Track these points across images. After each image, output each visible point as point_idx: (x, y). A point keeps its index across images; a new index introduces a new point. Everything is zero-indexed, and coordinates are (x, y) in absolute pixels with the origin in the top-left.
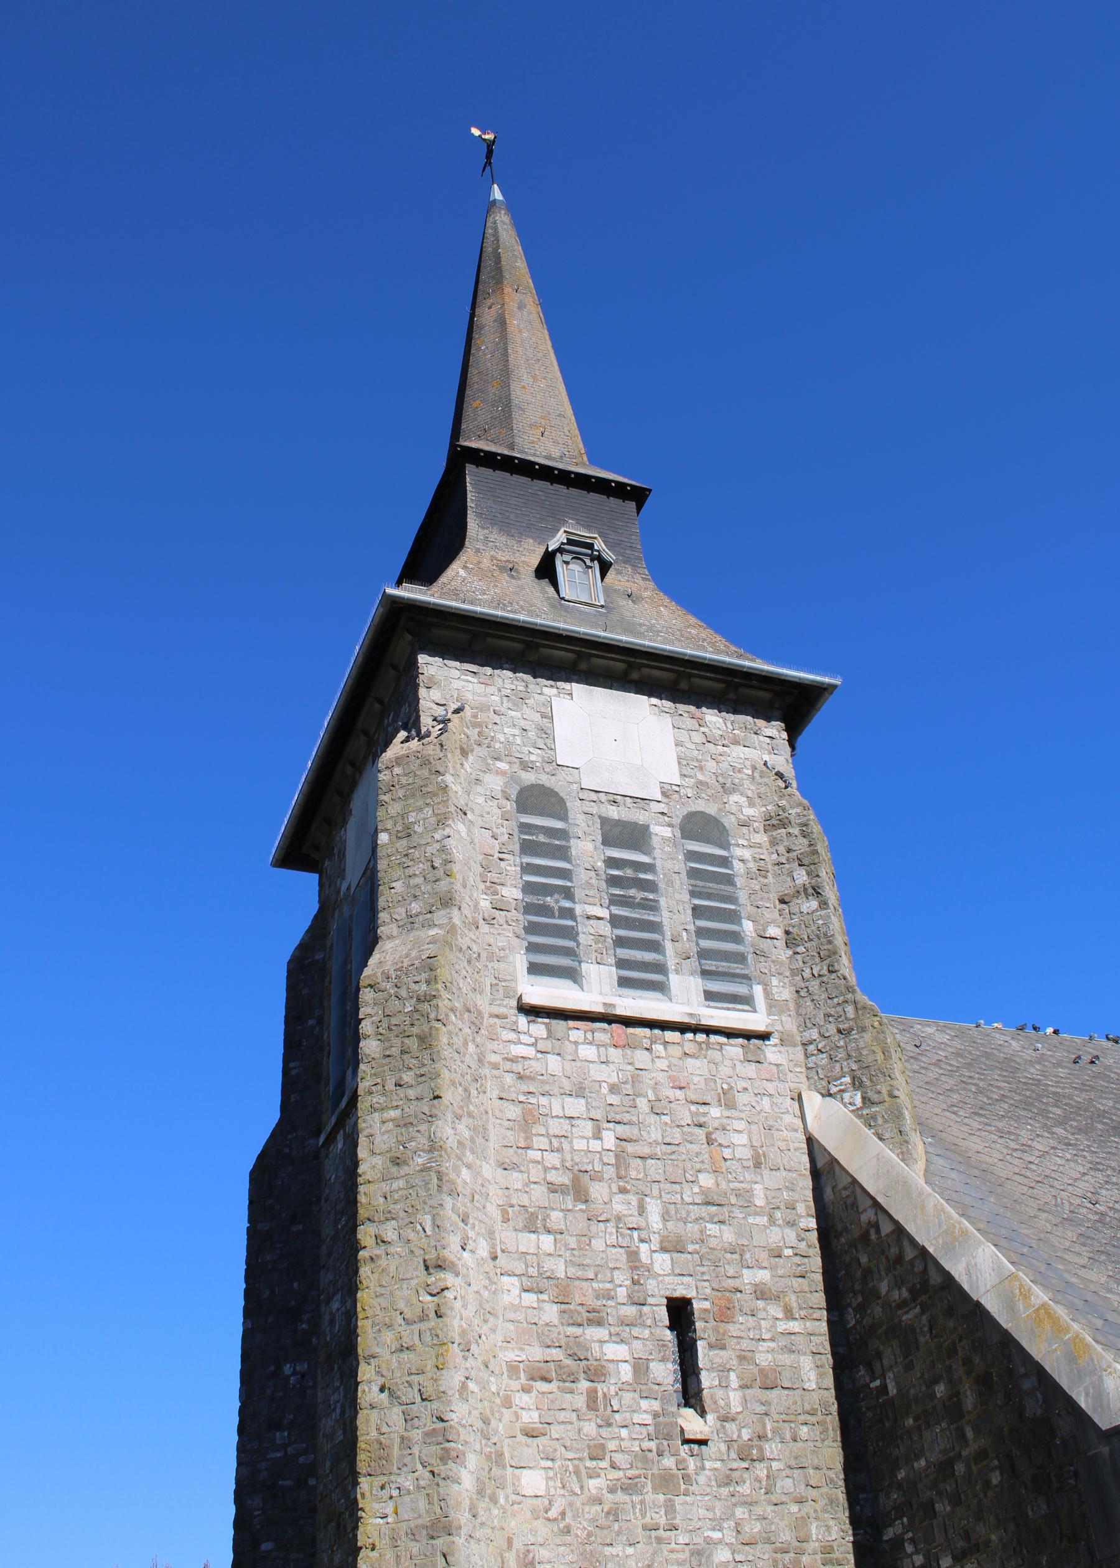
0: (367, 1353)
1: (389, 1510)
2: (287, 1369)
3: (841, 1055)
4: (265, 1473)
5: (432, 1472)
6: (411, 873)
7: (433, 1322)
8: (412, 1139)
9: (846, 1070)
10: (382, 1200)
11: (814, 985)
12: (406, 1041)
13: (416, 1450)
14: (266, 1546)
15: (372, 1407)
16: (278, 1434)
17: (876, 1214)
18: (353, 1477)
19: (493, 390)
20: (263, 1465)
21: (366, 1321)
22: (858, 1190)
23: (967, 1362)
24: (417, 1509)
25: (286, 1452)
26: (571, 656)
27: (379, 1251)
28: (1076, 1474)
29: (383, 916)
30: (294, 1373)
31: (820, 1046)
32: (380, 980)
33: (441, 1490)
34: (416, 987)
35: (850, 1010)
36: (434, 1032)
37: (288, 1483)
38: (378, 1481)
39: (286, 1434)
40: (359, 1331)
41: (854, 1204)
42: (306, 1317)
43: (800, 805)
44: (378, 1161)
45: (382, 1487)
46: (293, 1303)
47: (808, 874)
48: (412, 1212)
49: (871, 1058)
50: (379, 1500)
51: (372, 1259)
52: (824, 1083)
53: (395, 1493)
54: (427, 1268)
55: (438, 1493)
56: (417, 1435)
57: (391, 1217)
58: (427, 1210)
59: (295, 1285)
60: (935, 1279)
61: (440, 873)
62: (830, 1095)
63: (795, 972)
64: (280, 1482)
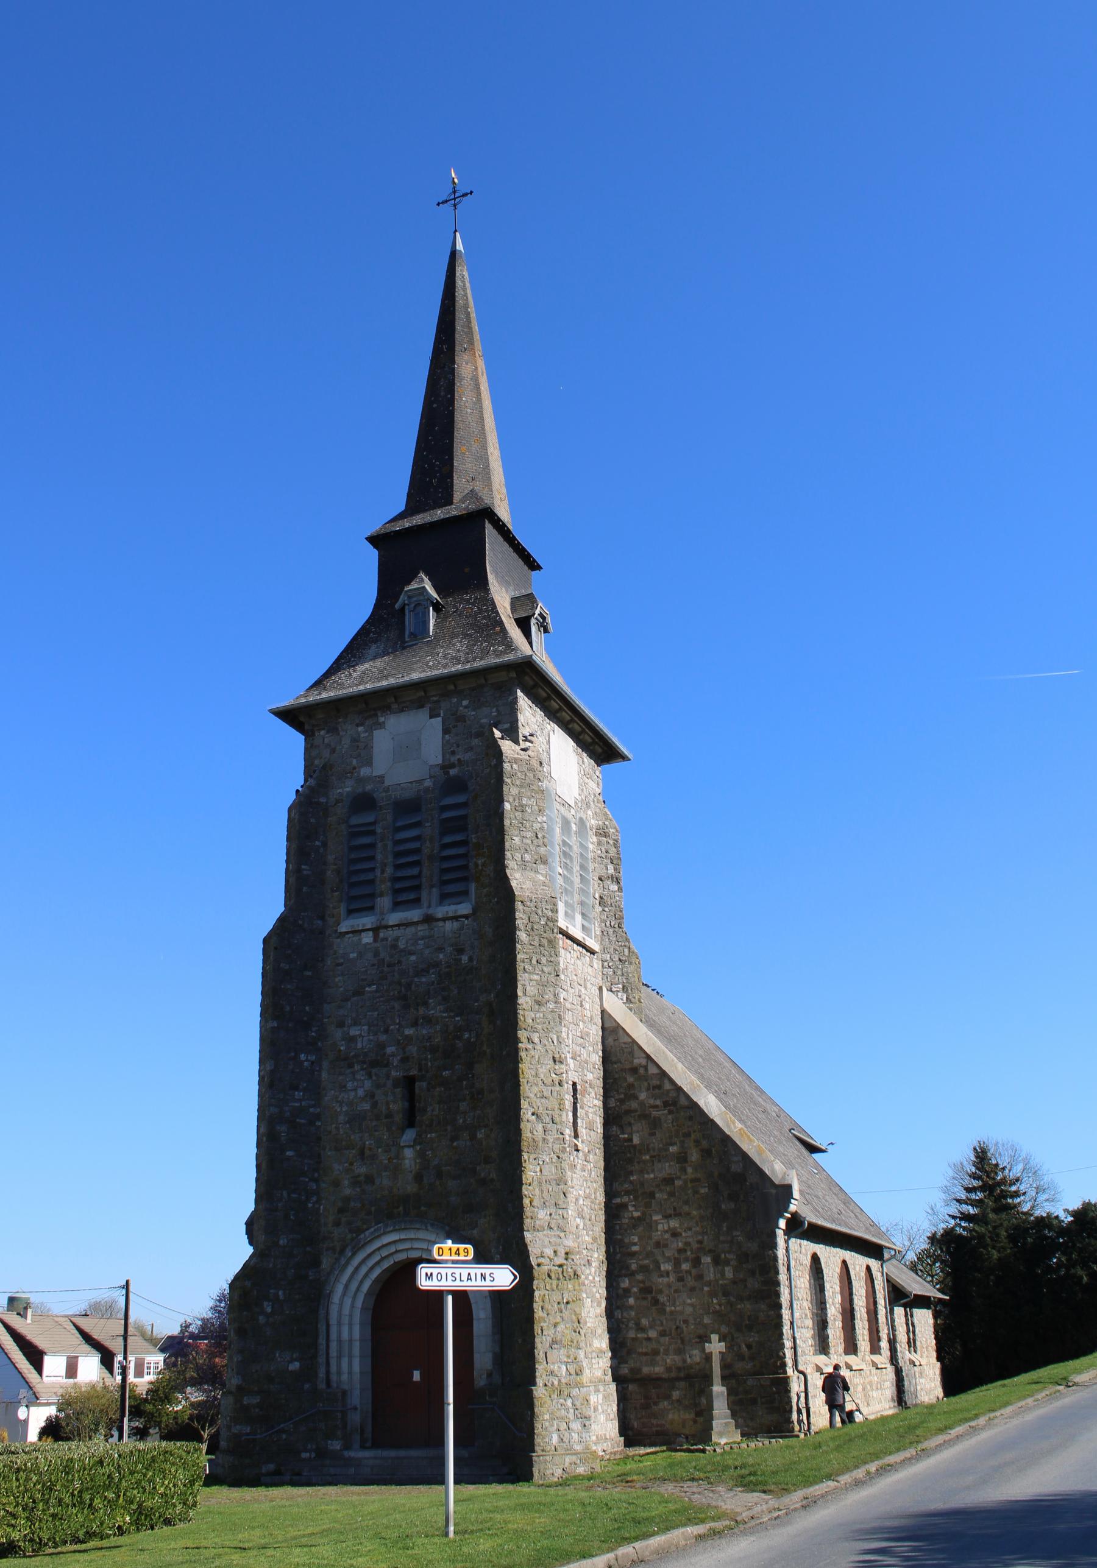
0: (525, 1095)
1: (538, 1170)
2: (303, 1057)
3: (619, 973)
4: (288, 1114)
5: (558, 1157)
6: (524, 835)
7: (558, 1088)
8: (546, 994)
9: (620, 981)
10: (531, 1021)
11: (611, 931)
12: (542, 940)
13: (550, 1145)
14: (289, 1153)
15: (528, 1121)
16: (296, 1093)
17: (647, 1062)
18: (519, 1152)
19: (475, 447)
20: (287, 1108)
21: (524, 1080)
22: (636, 1047)
23: (697, 1142)
24: (550, 1171)
25: (301, 1104)
26: (557, 707)
27: (530, 1046)
28: (754, 1197)
29: (508, 854)
30: (307, 1060)
31: (610, 964)
32: (526, 900)
33: (563, 1165)
34: (546, 911)
35: (626, 950)
36: (557, 940)
37: (303, 1121)
38: (533, 1156)
39: (301, 1094)
40: (521, 1084)
41: (632, 1053)
42: (314, 1029)
43: (615, 828)
44: (528, 999)
45: (535, 1159)
46: (305, 1019)
47: (615, 869)
48: (548, 1031)
49: (633, 979)
50: (533, 1165)
51: (526, 1050)
52: (609, 984)
53: (541, 1163)
54: (555, 1061)
55: (561, 1166)
56: (550, 1138)
57: (535, 1031)
58: (554, 1032)
59: (307, 1008)
60: (683, 1101)
61: (540, 842)
62: (612, 991)
63: (602, 921)
64: (298, 1120)
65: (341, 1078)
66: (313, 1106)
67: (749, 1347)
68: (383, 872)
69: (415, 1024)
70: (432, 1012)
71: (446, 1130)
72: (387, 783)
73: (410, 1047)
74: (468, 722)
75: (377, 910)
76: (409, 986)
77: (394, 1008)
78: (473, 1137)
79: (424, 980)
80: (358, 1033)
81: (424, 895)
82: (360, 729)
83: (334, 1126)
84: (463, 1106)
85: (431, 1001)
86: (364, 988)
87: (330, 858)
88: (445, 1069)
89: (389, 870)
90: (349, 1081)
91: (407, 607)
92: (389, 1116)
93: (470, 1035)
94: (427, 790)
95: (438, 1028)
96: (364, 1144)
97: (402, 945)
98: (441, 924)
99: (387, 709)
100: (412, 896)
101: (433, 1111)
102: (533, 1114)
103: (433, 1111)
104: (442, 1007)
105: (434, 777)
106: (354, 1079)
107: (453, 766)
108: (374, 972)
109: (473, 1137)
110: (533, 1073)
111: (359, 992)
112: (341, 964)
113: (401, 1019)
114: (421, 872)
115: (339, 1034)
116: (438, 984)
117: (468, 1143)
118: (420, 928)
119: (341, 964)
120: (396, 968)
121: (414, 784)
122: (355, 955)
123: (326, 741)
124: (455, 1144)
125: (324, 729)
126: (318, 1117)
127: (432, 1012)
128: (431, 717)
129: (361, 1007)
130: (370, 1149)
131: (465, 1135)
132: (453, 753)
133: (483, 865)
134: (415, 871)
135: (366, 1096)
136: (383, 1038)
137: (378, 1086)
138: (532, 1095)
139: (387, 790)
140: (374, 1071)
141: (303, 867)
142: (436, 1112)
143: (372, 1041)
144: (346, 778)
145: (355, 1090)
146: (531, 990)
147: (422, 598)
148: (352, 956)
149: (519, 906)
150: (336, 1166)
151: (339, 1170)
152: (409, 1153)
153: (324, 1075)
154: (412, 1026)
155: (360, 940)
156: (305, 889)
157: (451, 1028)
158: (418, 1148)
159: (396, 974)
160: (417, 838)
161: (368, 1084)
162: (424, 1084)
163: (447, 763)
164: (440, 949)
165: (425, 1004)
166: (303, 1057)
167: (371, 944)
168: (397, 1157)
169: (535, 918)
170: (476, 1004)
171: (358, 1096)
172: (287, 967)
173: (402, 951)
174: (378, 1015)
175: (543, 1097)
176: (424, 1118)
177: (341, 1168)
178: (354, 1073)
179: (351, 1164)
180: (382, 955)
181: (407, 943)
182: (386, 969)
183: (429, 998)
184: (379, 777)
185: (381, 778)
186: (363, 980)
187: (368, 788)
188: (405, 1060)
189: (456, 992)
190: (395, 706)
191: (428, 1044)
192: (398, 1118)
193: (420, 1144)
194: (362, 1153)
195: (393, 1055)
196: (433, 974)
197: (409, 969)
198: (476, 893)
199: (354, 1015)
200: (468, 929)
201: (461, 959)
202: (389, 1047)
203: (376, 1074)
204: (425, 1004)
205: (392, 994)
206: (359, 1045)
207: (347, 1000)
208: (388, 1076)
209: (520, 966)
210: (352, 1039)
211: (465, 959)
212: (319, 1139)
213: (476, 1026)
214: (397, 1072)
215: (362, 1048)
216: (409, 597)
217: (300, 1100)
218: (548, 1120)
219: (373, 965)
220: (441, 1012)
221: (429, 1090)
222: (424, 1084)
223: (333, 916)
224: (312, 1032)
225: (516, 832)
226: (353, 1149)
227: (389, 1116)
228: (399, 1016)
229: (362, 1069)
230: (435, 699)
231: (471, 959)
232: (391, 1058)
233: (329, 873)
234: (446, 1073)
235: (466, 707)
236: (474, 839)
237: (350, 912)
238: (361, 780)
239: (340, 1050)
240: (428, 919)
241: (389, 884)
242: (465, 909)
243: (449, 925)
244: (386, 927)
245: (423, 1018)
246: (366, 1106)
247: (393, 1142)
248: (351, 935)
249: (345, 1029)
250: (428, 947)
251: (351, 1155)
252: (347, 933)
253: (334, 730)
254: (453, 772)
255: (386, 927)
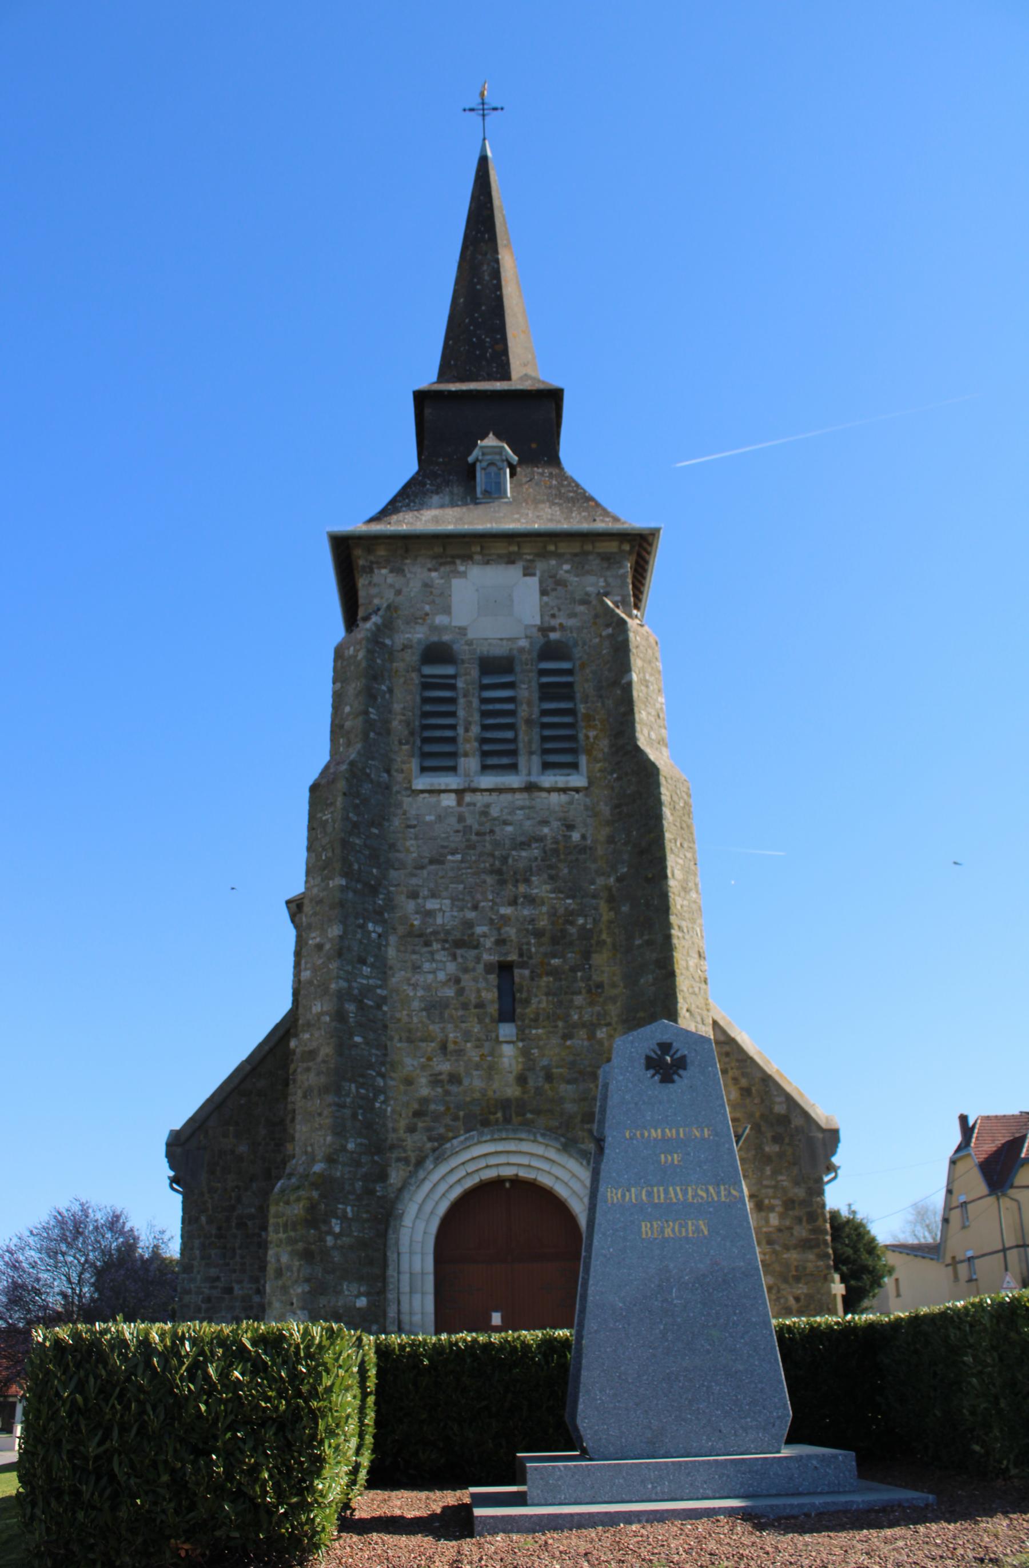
2: (370, 926)
14: (358, 1039)
27: (680, 935)
28: (800, 1140)
37: (370, 1003)
42: (381, 896)
46: (373, 882)
54: (700, 956)
65: (414, 957)
66: (380, 987)
67: (797, 1299)
68: (467, 730)
69: (513, 902)
70: (535, 891)
71: (556, 1027)
72: (471, 635)
73: (508, 929)
74: (570, 588)
75: (461, 770)
76: (504, 859)
77: (485, 882)
78: (592, 1036)
79: (524, 854)
80: (437, 906)
81: (522, 761)
82: (434, 574)
83: (405, 1013)
84: (579, 1000)
85: (534, 878)
86: (446, 857)
87: (397, 707)
88: (554, 956)
89: (475, 730)
90: (426, 961)
91: (478, 464)
92: (480, 1005)
93: (586, 920)
94: (521, 650)
95: (544, 909)
96: (447, 1036)
97: (495, 812)
98: (544, 795)
99: (468, 558)
100: (505, 761)
101: (539, 1002)
102: (688, 1010)
103: (539, 1002)
104: (548, 887)
105: (531, 637)
106: (433, 960)
107: (553, 629)
108: (457, 839)
109: (592, 1036)
110: (685, 966)
111: (437, 860)
112: (414, 827)
113: (495, 895)
114: (516, 736)
115: (411, 906)
116: (543, 860)
117: (586, 1043)
118: (518, 796)
119: (414, 827)
120: (488, 838)
121: (505, 642)
122: (433, 818)
123: (390, 580)
124: (568, 1043)
125: (385, 567)
126: (384, 1000)
127: (535, 891)
128: (525, 575)
129: (442, 877)
130: (455, 1043)
131: (583, 1033)
132: (553, 616)
133: (596, 737)
134: (509, 735)
135: (450, 980)
136: (471, 915)
137: (466, 970)
138: (685, 989)
139: (470, 643)
140: (459, 952)
141: (371, 710)
142: (543, 1005)
143: (456, 917)
144: (416, 623)
145: (434, 972)
146: (679, 874)
147: (497, 457)
148: (428, 818)
149: (662, 780)
150: (408, 1061)
151: (413, 1065)
152: (508, 1050)
153: (391, 952)
154: (510, 904)
155: (439, 802)
156: (372, 735)
157: (561, 911)
158: (520, 1044)
159: (487, 844)
160: (511, 700)
161: (451, 967)
162: (526, 972)
163: (546, 625)
164: (545, 822)
165: (527, 881)
166: (370, 926)
167: (452, 807)
168: (492, 1054)
169: (675, 798)
170: (593, 887)
171: (439, 979)
172: (355, 819)
173: (495, 819)
174: (465, 888)
175: (694, 993)
176: (527, 1011)
177: (415, 1063)
178: (432, 953)
179: (429, 1059)
180: (469, 821)
181: (502, 811)
182: (474, 837)
183: (531, 875)
184: (460, 628)
185: (462, 631)
186: (443, 847)
187: (446, 638)
188: (501, 942)
189: (566, 871)
190: (477, 557)
191: (530, 927)
192: (493, 1009)
193: (522, 1040)
194: (443, 1047)
195: (485, 936)
196: (536, 848)
197: (504, 840)
198: (588, 767)
199: (432, 885)
200: (579, 804)
201: (570, 837)
202: (479, 925)
203: (462, 956)
204: (527, 881)
205: (482, 865)
206: (439, 921)
207: (422, 867)
208: (478, 959)
209: (669, 845)
210: (430, 914)
211: (576, 836)
212: (385, 1027)
213: (593, 912)
214: (490, 955)
215: (443, 925)
216: (483, 454)
217: (367, 977)
218: (699, 1019)
219: (457, 831)
220: (547, 892)
221: (532, 979)
222: (526, 972)
223: (402, 771)
224: (379, 899)
225: (643, 707)
226: (432, 1041)
227: (480, 1005)
228: (493, 892)
229: (444, 949)
230: (528, 557)
231: (584, 837)
232: (482, 939)
233: (395, 724)
234: (555, 962)
235: (567, 572)
236: (582, 708)
237: (424, 769)
238: (434, 629)
239: (412, 925)
240: (531, 788)
241: (476, 744)
242: (578, 780)
243: (554, 797)
244: (475, 790)
245: (525, 897)
246: (450, 992)
247: (487, 1036)
248: (426, 795)
249: (420, 901)
250: (528, 819)
251: (429, 1049)
252: (422, 791)
253: (399, 571)
254: (554, 636)
255: (475, 790)
